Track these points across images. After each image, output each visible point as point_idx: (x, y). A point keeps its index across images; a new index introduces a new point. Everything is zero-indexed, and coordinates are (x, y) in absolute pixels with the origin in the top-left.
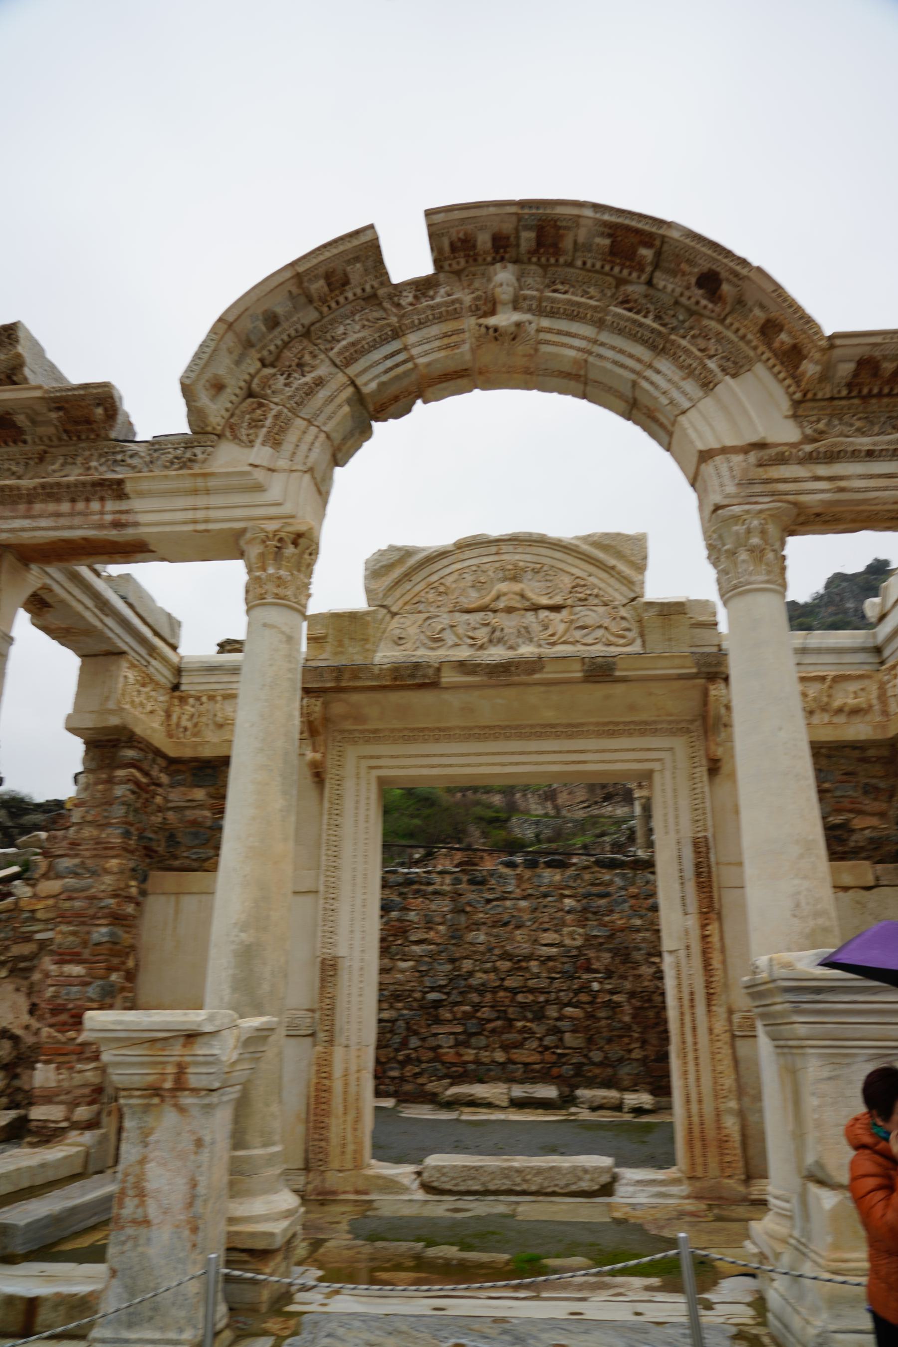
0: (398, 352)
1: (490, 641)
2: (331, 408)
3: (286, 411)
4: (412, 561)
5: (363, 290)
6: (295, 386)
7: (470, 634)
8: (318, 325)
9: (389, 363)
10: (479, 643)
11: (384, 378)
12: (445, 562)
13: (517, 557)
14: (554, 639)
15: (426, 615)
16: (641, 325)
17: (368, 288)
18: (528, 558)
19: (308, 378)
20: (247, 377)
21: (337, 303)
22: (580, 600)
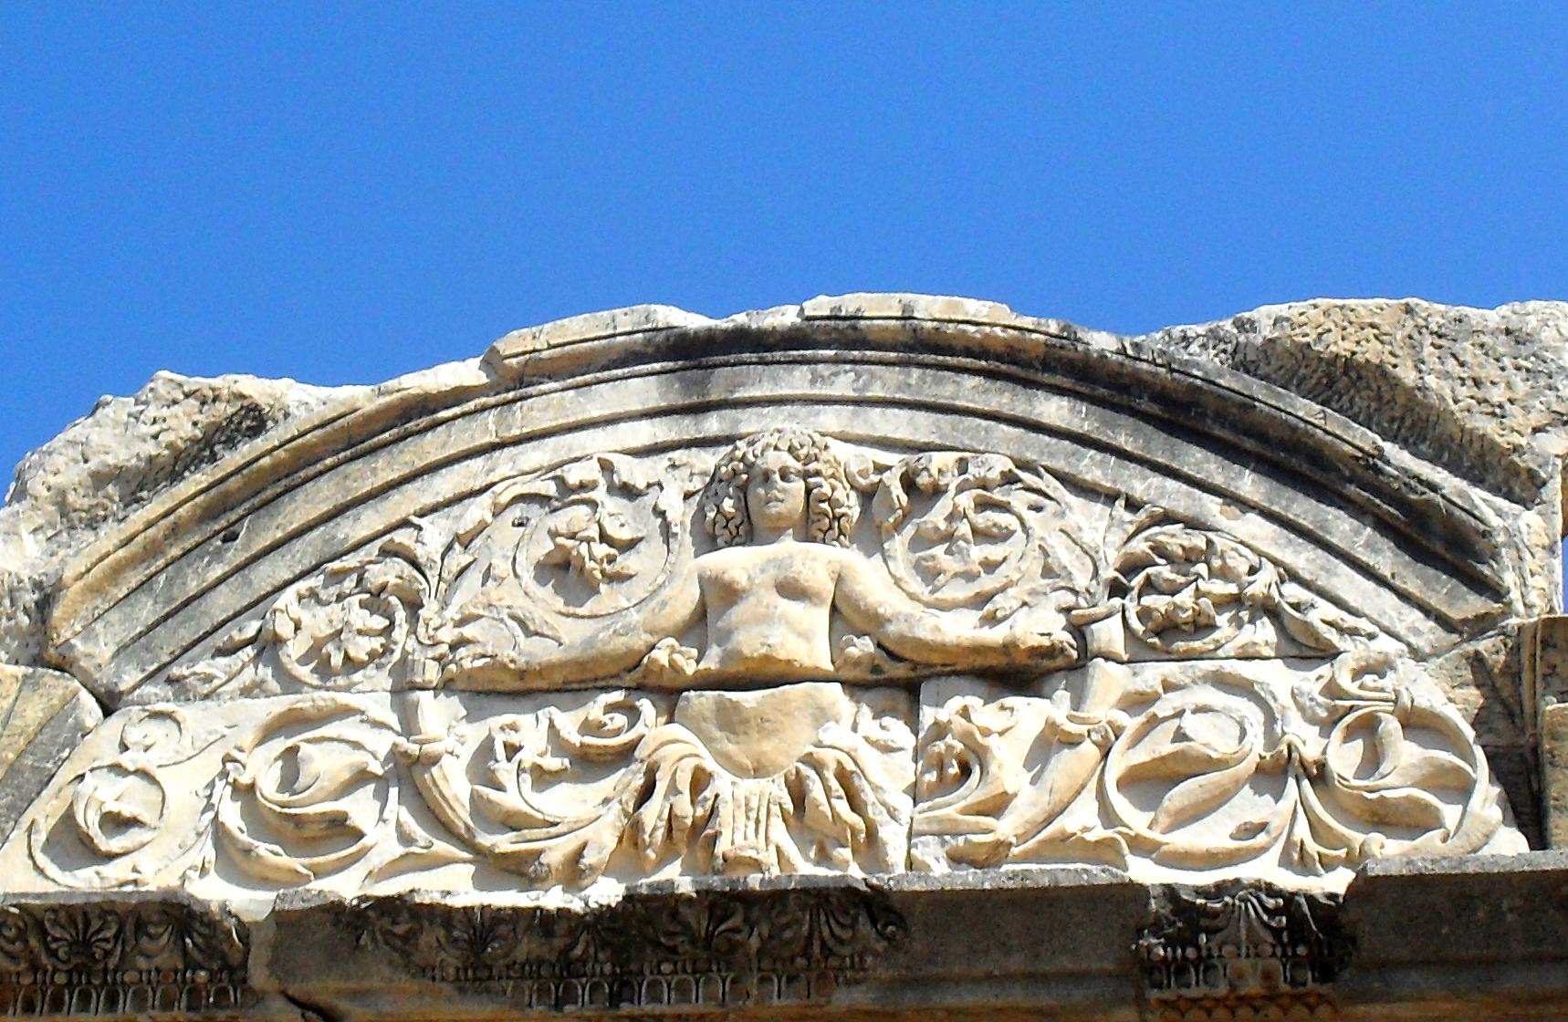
7: (510, 799)
12: (432, 446)
13: (831, 419)
14: (1005, 828)
15: (279, 704)
22: (1168, 628)
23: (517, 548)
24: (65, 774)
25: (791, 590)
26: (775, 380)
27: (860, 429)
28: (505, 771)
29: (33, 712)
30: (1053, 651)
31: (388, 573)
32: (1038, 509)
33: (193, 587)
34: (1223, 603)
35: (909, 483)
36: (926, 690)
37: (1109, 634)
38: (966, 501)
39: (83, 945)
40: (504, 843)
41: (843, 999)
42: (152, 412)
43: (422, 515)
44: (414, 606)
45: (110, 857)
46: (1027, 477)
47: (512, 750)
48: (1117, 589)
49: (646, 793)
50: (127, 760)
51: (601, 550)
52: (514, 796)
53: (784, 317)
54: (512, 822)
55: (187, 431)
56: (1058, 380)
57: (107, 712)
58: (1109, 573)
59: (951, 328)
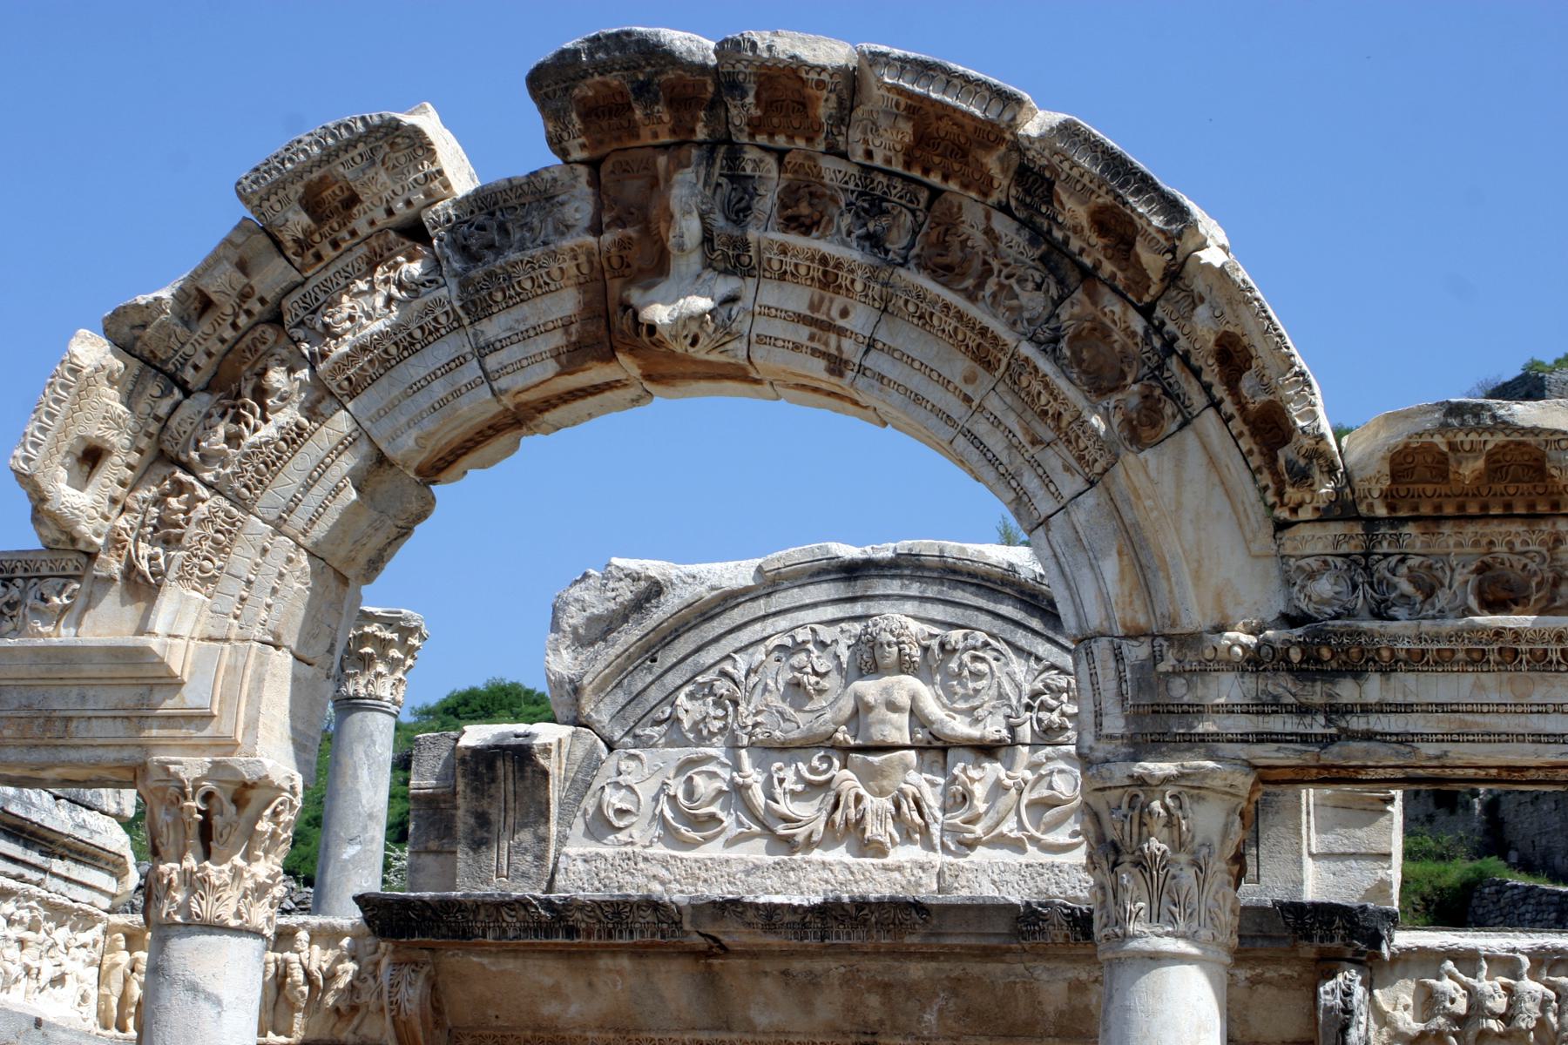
0: (460, 361)
1: (830, 823)
2: (318, 492)
3: (226, 504)
4: (660, 613)
5: (390, 212)
6: (250, 438)
8: (296, 296)
9: (439, 389)
10: (801, 834)
11: (429, 424)
13: (910, 607)
14: (978, 830)
16: (960, 316)
17: (399, 205)
18: (937, 612)
19: (268, 431)
20: (154, 427)
21: (335, 245)
23: (778, 676)
24: (596, 785)
25: (893, 707)
26: (885, 586)
27: (922, 615)
28: (778, 791)
29: (579, 753)
30: (1000, 741)
31: (723, 687)
32: (997, 659)
33: (640, 686)
34: (1071, 717)
35: (942, 645)
36: (950, 753)
37: (1025, 733)
38: (966, 658)
39: (617, 914)
40: (781, 829)
41: (908, 940)
42: (611, 585)
43: (736, 652)
44: (736, 703)
45: (620, 829)
46: (991, 641)
47: (781, 781)
48: (1029, 708)
49: (836, 806)
50: (621, 779)
51: (813, 679)
52: (785, 806)
53: (885, 552)
54: (786, 819)
55: (629, 596)
56: (1008, 590)
57: (611, 747)
58: (1025, 700)
59: (960, 563)
